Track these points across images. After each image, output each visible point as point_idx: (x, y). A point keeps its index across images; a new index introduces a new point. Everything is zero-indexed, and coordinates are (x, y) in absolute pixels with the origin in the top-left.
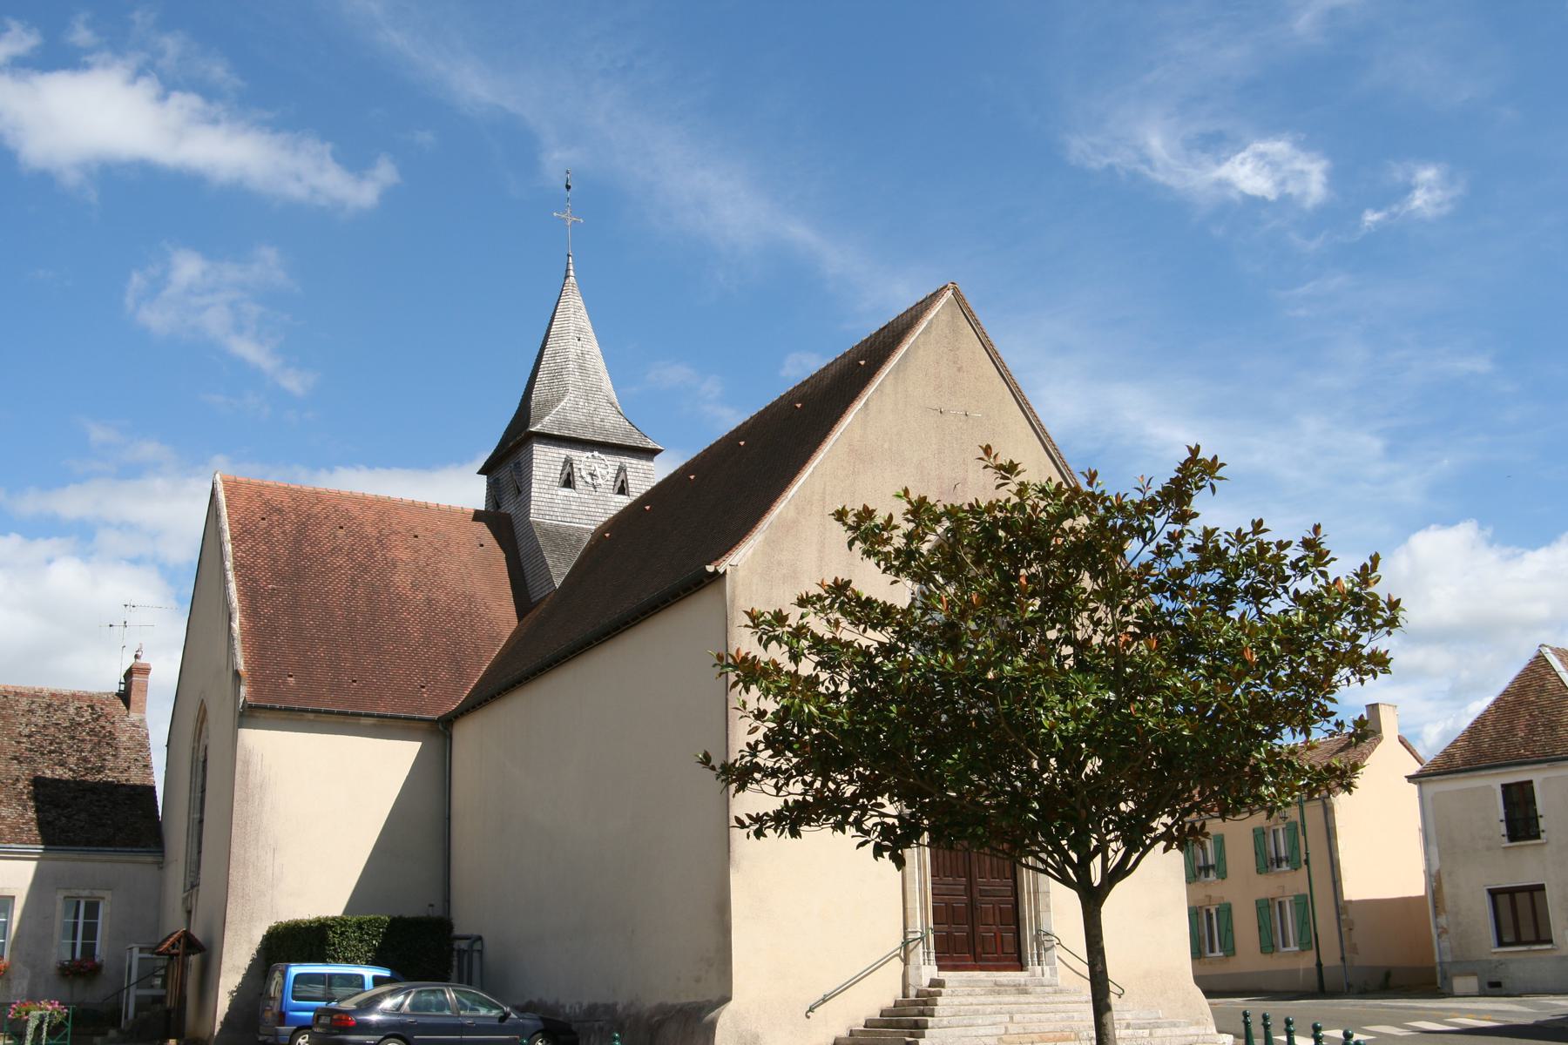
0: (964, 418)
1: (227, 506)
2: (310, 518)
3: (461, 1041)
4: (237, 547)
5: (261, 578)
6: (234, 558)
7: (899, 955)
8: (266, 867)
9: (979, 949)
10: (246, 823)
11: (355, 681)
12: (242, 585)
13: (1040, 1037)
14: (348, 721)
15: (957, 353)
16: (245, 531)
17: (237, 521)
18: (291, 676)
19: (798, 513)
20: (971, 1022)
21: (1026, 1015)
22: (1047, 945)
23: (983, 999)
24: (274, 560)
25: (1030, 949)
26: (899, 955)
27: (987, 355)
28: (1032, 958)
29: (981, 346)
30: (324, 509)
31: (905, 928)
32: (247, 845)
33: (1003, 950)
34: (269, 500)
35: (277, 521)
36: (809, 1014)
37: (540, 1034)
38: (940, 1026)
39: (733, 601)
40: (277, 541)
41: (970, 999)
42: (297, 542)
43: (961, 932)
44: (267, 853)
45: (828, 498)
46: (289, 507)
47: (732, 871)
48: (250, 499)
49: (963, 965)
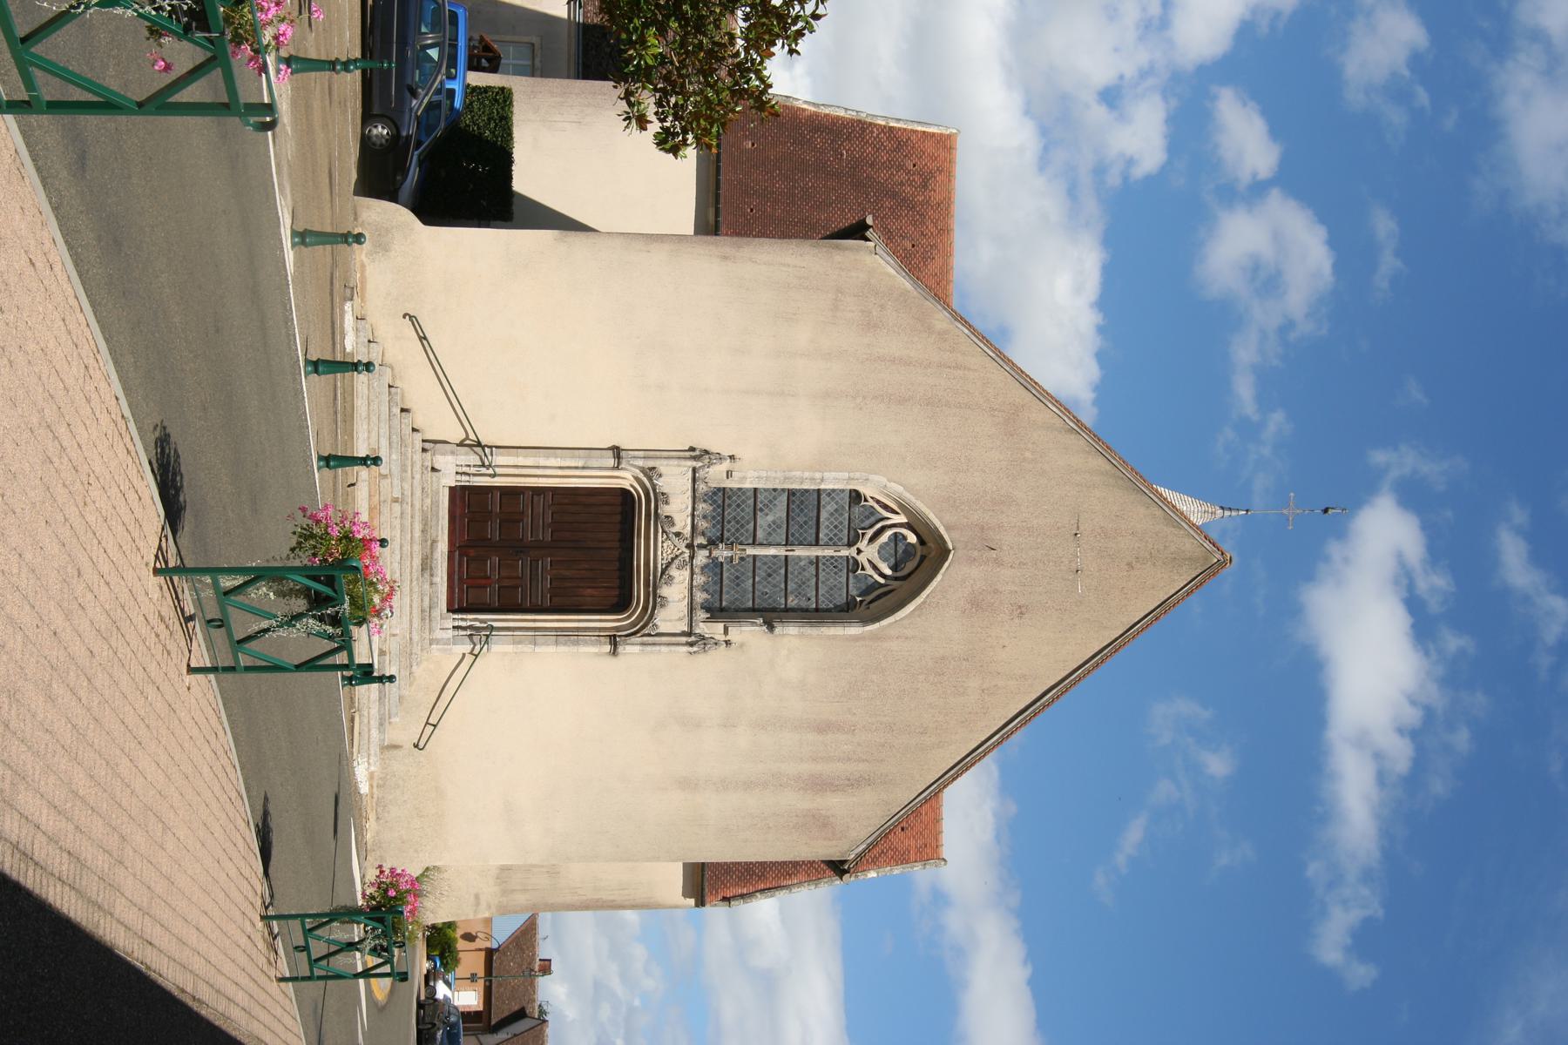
0: (1074, 566)
1: (924, 132)
2: (920, 215)
3: (392, 43)
4: (882, 130)
5: (852, 146)
6: (870, 124)
7: (467, 438)
8: (563, 114)
9: (472, 552)
10: (605, 94)
11: (752, 210)
12: (843, 123)
13: (375, 508)
14: (711, 194)
15: (1149, 563)
16: (899, 144)
17: (909, 138)
18: (753, 145)
19: (939, 334)
20: (394, 445)
21: (398, 521)
22: (476, 639)
23: (418, 505)
24: (872, 165)
25: (471, 619)
26: (467, 438)
27: (1153, 608)
28: (462, 619)
29: (1163, 600)
30: (932, 234)
31: (497, 447)
32: (583, 96)
33: (472, 587)
34: (935, 178)
35: (914, 180)
36: (407, 317)
37: (395, 132)
38: (391, 404)
39: (837, 247)
40: (892, 173)
41: (418, 493)
42: (894, 195)
43: (493, 531)
44: (576, 115)
45: (960, 372)
46: (930, 197)
47: (556, 232)
48: (934, 158)
49: (455, 528)
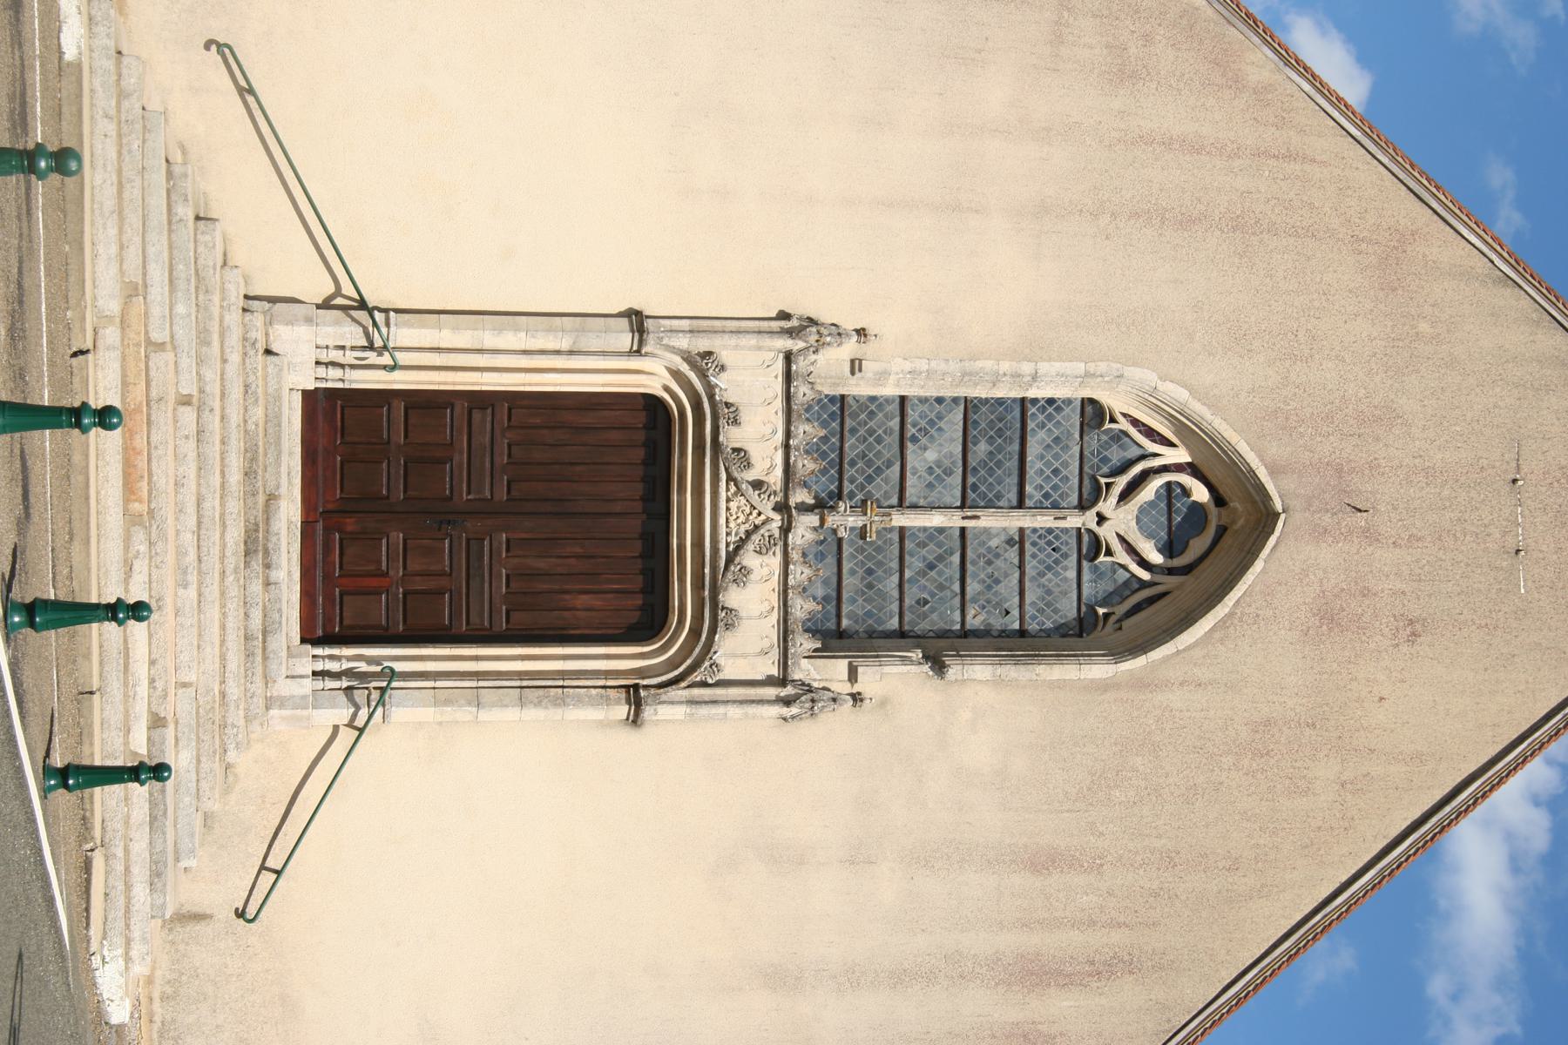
0: (1511, 544)
7: (338, 292)
9: (351, 524)
20: (182, 285)
21: (192, 444)
22: (360, 696)
23: (235, 418)
26: (338, 292)
28: (331, 657)
31: (397, 311)
36: (214, 48)
38: (174, 197)
41: (236, 392)
43: (390, 481)
45: (1295, 168)
